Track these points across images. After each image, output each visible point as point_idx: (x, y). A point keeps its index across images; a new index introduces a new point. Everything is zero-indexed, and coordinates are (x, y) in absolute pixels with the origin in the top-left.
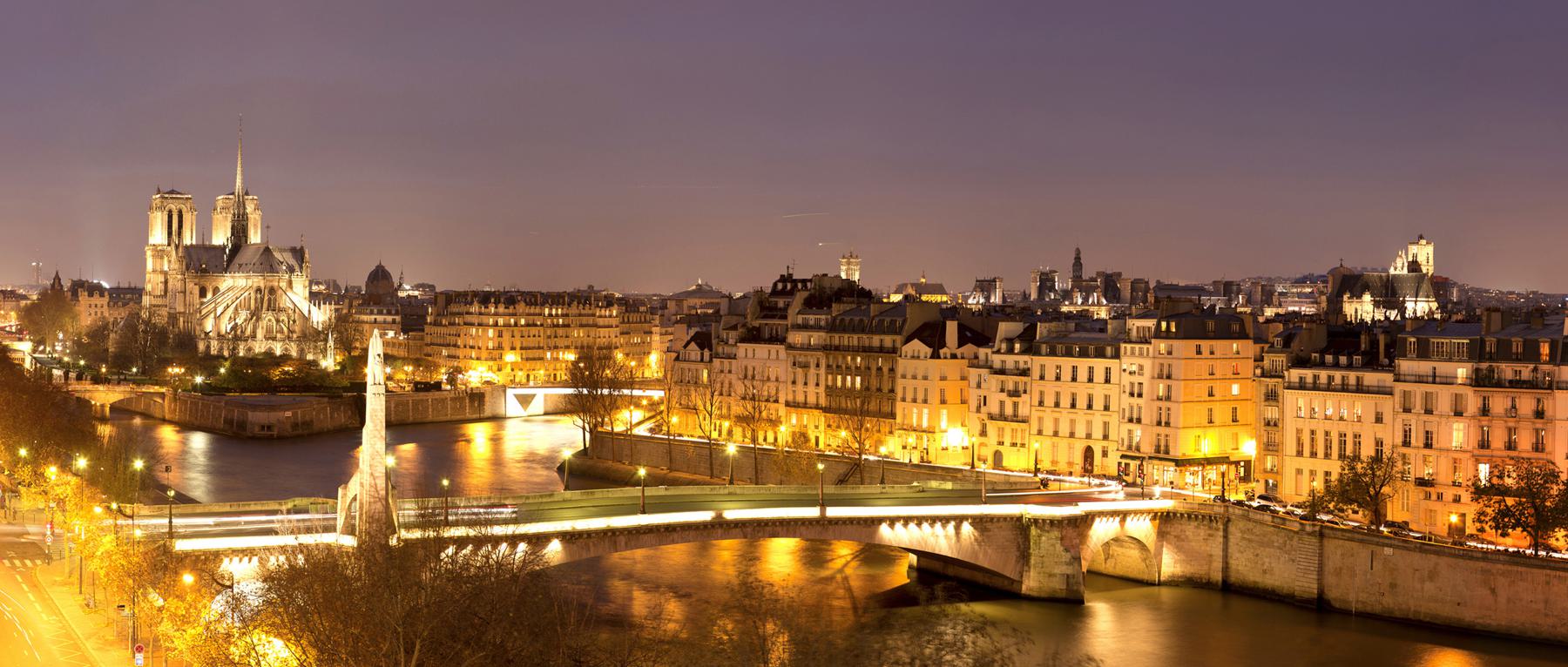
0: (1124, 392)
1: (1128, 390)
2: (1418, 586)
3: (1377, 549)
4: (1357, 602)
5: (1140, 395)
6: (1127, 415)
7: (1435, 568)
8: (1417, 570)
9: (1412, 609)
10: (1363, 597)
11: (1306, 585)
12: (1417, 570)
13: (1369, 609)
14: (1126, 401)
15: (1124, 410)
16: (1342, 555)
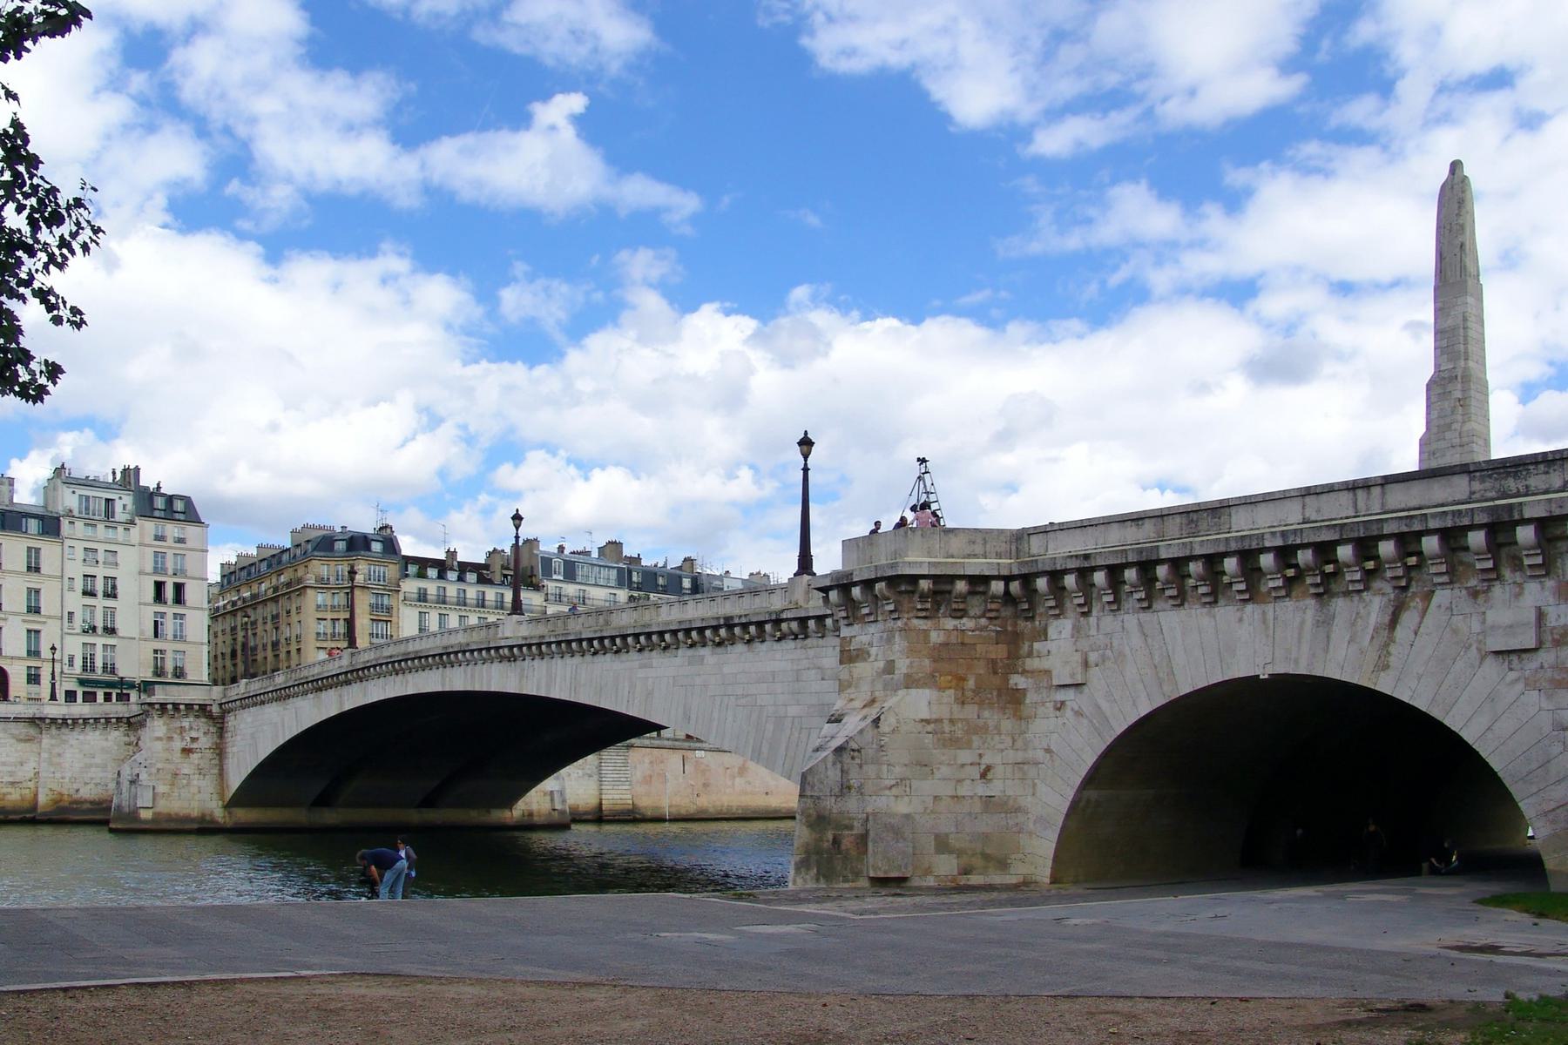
0: (71, 589)
1: (79, 585)
2: (729, 783)
3: (689, 754)
4: (670, 807)
5: (111, 594)
6: (78, 623)
7: (744, 765)
8: (728, 768)
9: (726, 804)
10: (677, 800)
11: (618, 797)
12: (728, 768)
13: (683, 812)
14: (75, 602)
15: (71, 614)
16: (651, 762)
